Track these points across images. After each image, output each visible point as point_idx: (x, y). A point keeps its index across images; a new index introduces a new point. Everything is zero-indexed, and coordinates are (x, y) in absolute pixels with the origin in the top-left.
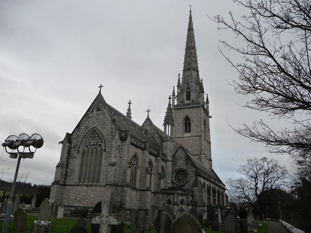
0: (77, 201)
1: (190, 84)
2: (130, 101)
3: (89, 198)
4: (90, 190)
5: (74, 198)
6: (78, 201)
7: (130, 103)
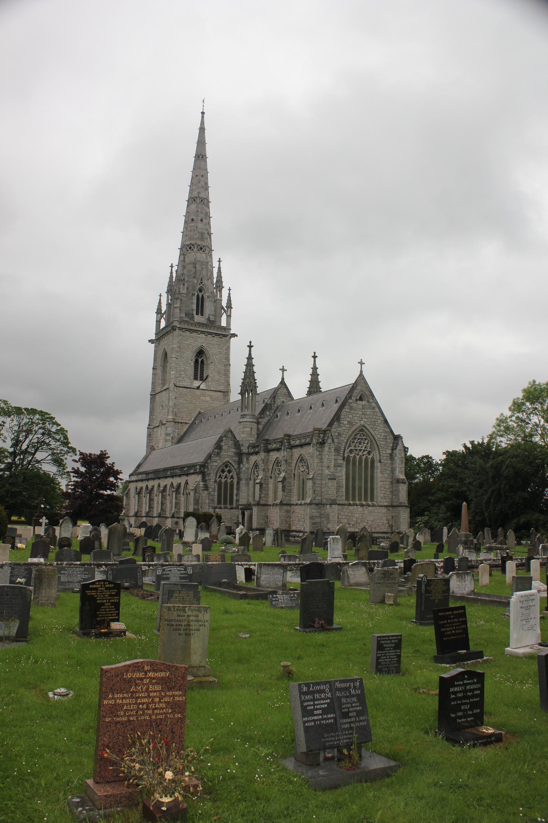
0: (351, 525)
1: (205, 282)
2: (250, 342)
3: (366, 521)
4: (366, 510)
5: (346, 521)
6: (353, 525)
7: (250, 347)
